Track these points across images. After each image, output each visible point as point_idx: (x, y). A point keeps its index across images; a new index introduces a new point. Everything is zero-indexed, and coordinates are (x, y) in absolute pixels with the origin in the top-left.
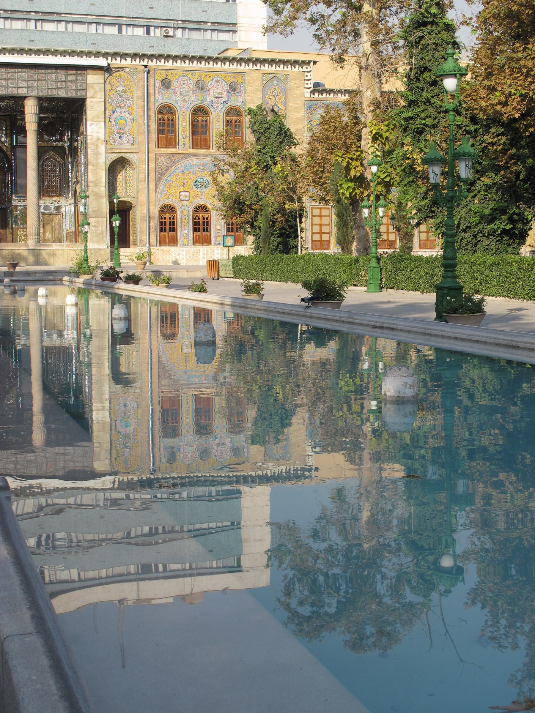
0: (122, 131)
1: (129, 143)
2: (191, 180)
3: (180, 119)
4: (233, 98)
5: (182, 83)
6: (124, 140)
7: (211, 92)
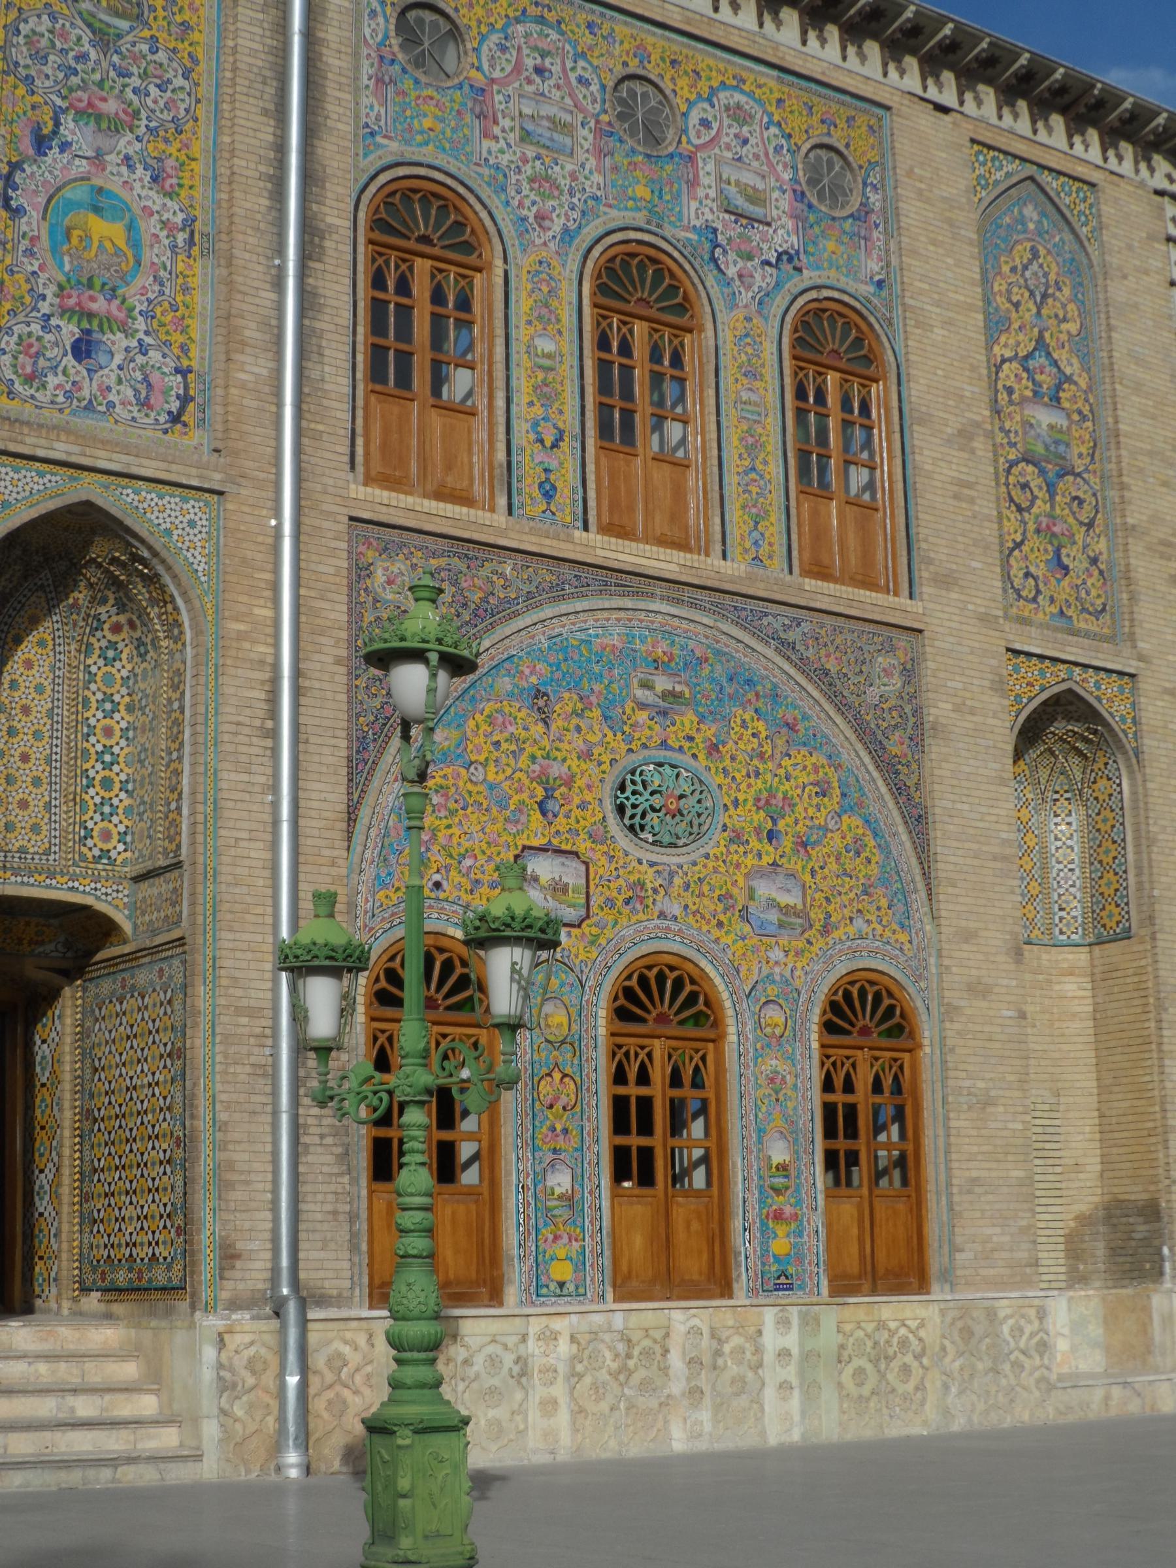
0: (99, 305)
1: (145, 404)
2: (590, 766)
3: (522, 304)
4: (831, 245)
5: (529, 63)
6: (109, 375)
7: (706, 169)
